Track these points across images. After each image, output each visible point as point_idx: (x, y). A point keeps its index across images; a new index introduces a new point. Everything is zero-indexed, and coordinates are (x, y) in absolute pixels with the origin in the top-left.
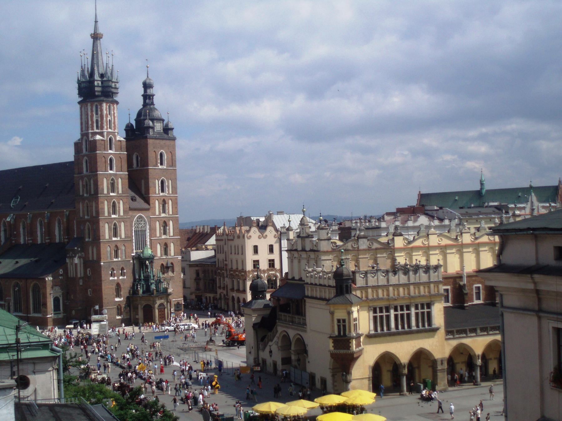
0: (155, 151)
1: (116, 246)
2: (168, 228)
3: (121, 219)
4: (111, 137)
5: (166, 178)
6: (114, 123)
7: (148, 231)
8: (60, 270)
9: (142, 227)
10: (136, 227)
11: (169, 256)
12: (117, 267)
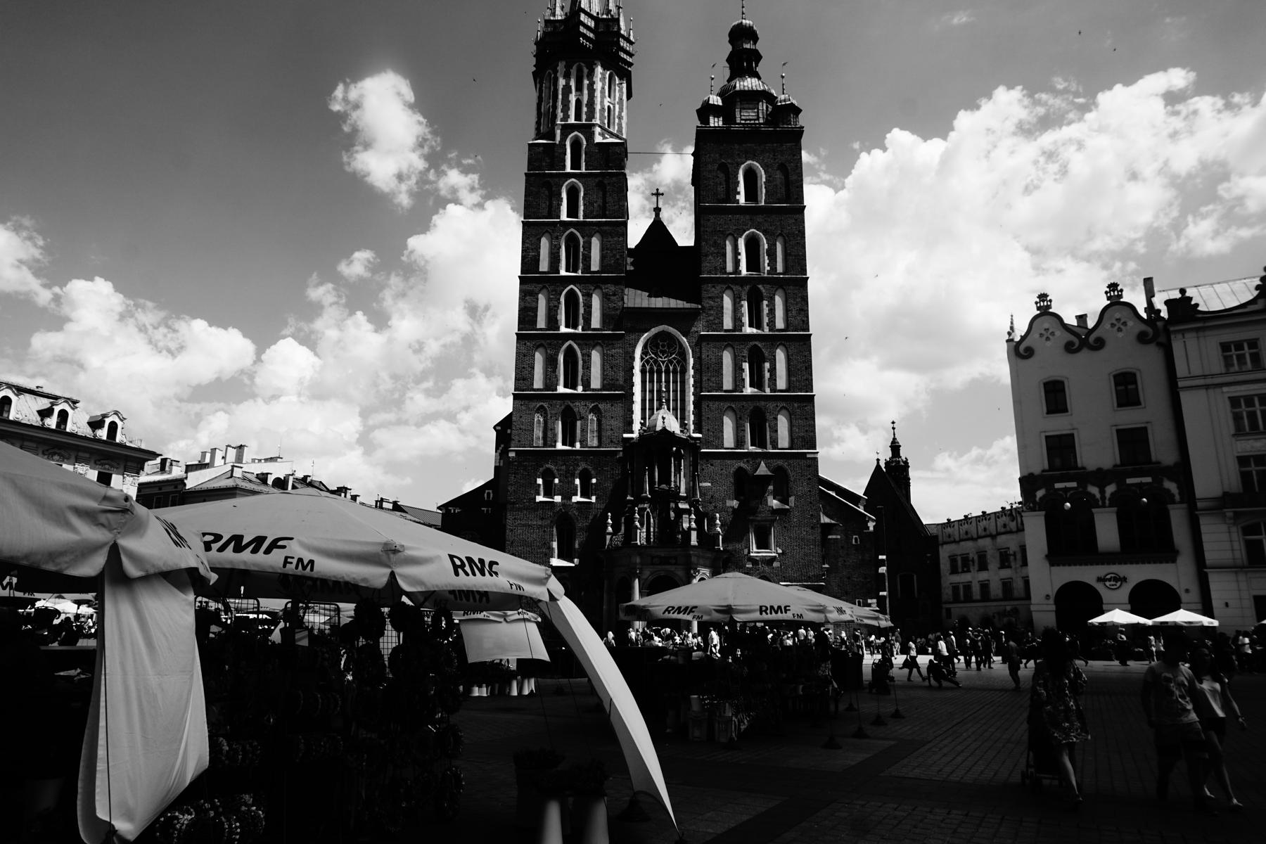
1: (568, 408)
2: (767, 365)
3: (589, 340)
4: (576, 137)
5: (765, 233)
7: (692, 372)
8: (487, 491)
9: (670, 362)
10: (647, 361)
11: (769, 445)
12: (564, 467)
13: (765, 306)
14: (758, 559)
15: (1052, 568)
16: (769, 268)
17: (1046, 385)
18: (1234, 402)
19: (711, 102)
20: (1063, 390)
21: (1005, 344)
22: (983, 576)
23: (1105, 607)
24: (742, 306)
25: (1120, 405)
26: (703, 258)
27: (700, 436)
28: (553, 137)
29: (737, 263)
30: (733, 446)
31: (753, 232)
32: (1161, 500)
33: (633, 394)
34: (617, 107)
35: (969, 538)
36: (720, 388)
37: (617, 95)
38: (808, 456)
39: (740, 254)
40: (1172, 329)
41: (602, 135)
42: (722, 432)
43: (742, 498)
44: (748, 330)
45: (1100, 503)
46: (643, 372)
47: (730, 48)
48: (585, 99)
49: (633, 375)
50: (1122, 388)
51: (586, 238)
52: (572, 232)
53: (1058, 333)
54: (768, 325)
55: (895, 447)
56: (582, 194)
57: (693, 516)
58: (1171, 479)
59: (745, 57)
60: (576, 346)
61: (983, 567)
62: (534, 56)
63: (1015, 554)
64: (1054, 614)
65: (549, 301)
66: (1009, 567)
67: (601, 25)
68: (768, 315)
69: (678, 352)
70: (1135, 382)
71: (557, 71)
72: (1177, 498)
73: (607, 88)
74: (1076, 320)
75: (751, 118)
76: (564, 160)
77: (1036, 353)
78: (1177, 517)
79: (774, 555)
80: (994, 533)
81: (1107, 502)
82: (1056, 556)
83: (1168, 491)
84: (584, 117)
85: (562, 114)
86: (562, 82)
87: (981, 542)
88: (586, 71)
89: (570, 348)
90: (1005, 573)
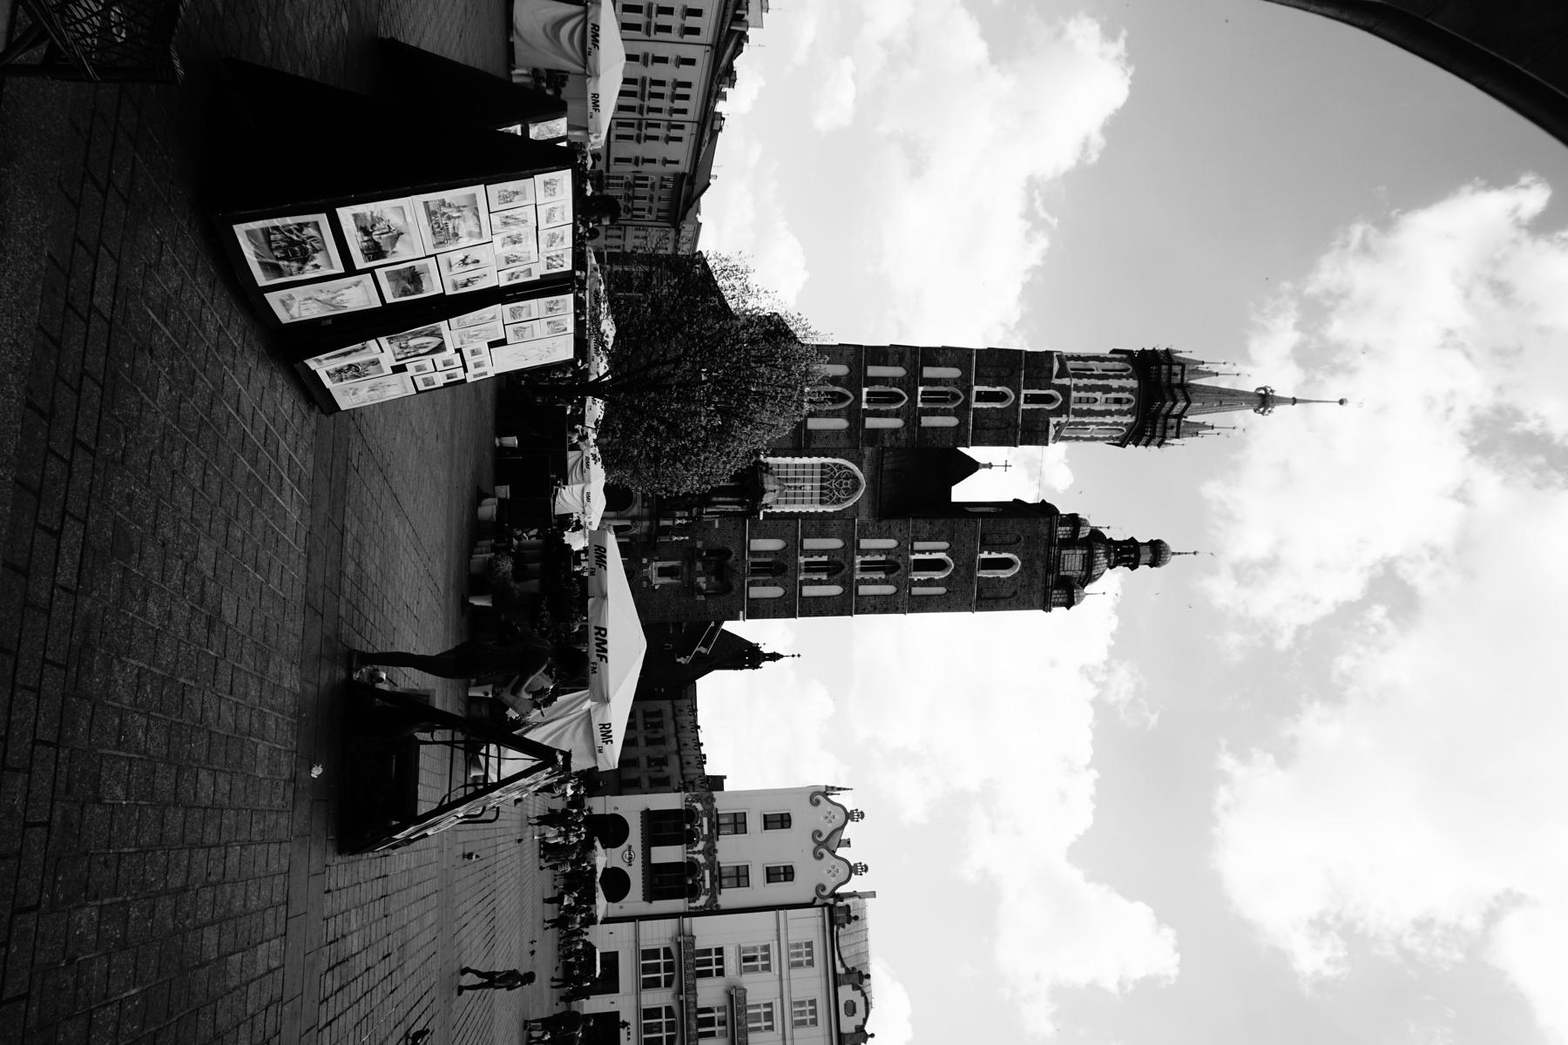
0: (1019, 540)
2: (824, 577)
3: (855, 416)
4: (1058, 400)
5: (950, 577)
6: (1090, 413)
7: (820, 510)
9: (831, 490)
10: (832, 470)
11: (751, 579)
13: (880, 576)
14: (650, 568)
15: (639, 815)
16: (916, 580)
17: (788, 814)
18: (766, 948)
19: (1081, 528)
20: (783, 827)
21: (824, 784)
22: (642, 742)
23: (609, 850)
24: (881, 556)
25: (768, 868)
26: (928, 521)
27: (761, 518)
28: (1058, 376)
29: (923, 552)
30: (752, 548)
31: (951, 566)
32: (693, 893)
33: (801, 457)
34: (1089, 436)
35: (678, 728)
36: (806, 535)
37: (1101, 436)
38: (741, 613)
39: (930, 554)
40: (826, 909)
41: (1058, 424)
42: (765, 538)
43: (705, 554)
44: (858, 559)
45: (690, 850)
46: (823, 466)
47: (1142, 538)
48: (1096, 407)
49: (819, 457)
50: (782, 871)
51: (953, 411)
52: (960, 397)
53: (830, 825)
54: (862, 578)
55: (775, 657)
56: (998, 405)
57: (684, 522)
58: (707, 901)
59: (1132, 556)
60: (848, 403)
61: (649, 742)
62: (1154, 349)
63: (661, 771)
64: (602, 812)
65: (894, 378)
66: (649, 766)
67: (1173, 421)
68: (871, 578)
69: (839, 498)
70: (786, 880)
71: (1128, 379)
72: (692, 905)
73: (1108, 427)
74: (846, 838)
75: (1066, 564)
76: (1033, 388)
77: (820, 806)
78: (678, 905)
79: (654, 582)
80: (682, 753)
81: (690, 856)
82: (649, 816)
83: (698, 899)
84: (1077, 407)
85: (1081, 385)
86: (1115, 383)
87: (673, 742)
88: (1125, 407)
89: (847, 398)
90: (643, 761)
